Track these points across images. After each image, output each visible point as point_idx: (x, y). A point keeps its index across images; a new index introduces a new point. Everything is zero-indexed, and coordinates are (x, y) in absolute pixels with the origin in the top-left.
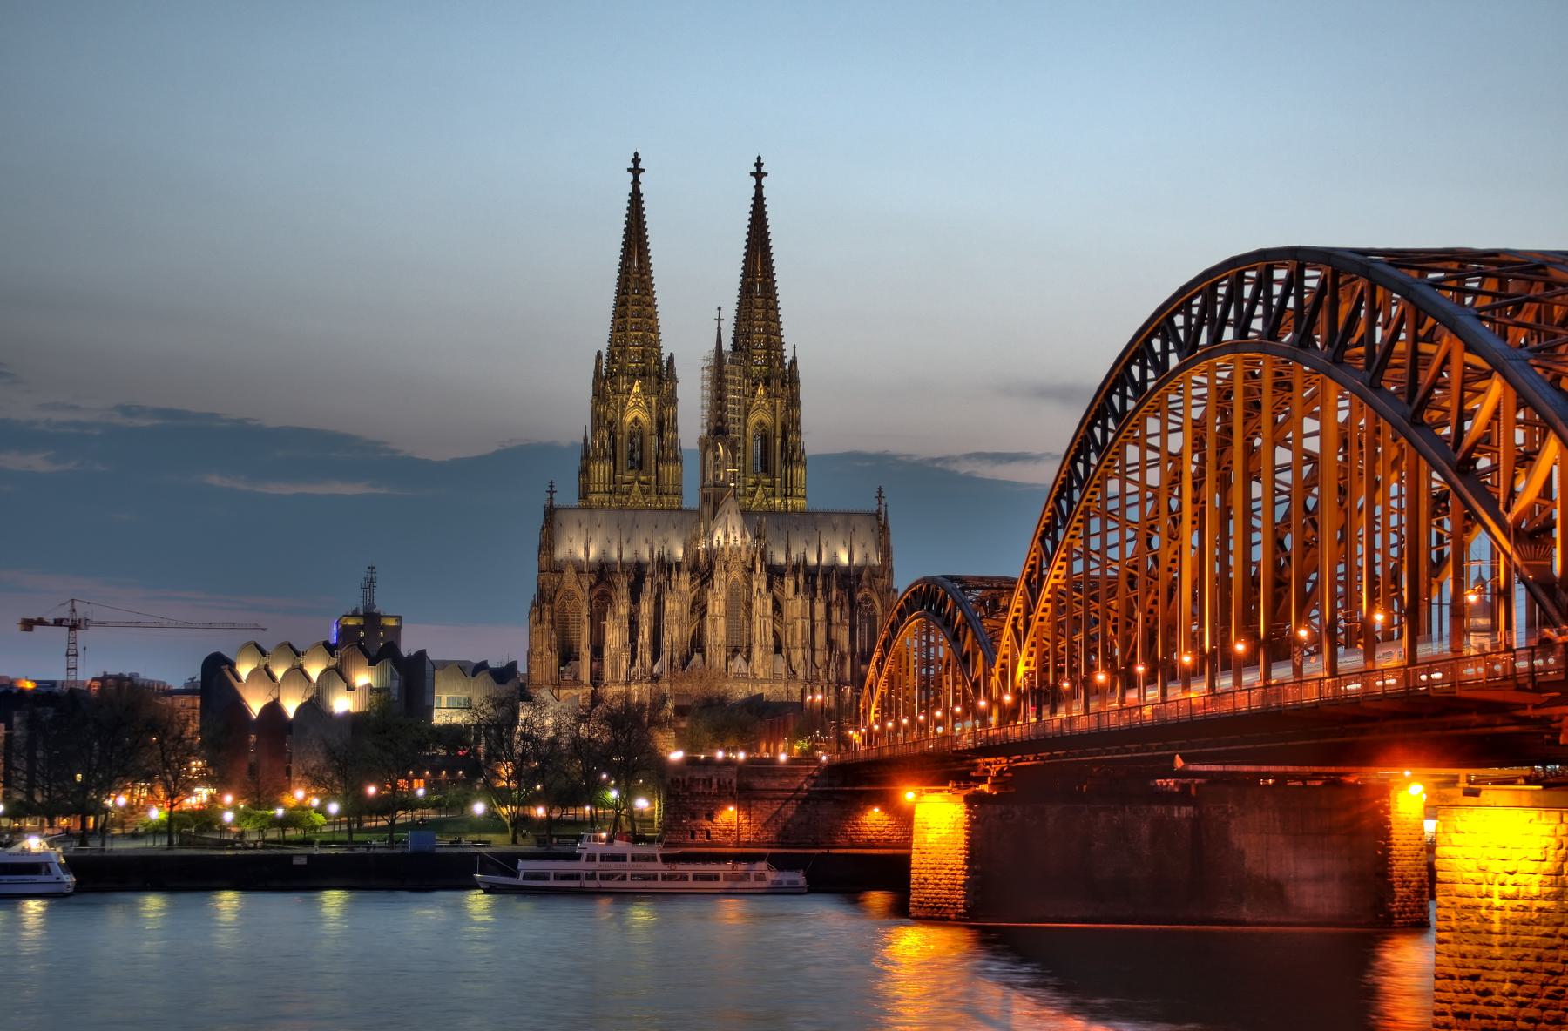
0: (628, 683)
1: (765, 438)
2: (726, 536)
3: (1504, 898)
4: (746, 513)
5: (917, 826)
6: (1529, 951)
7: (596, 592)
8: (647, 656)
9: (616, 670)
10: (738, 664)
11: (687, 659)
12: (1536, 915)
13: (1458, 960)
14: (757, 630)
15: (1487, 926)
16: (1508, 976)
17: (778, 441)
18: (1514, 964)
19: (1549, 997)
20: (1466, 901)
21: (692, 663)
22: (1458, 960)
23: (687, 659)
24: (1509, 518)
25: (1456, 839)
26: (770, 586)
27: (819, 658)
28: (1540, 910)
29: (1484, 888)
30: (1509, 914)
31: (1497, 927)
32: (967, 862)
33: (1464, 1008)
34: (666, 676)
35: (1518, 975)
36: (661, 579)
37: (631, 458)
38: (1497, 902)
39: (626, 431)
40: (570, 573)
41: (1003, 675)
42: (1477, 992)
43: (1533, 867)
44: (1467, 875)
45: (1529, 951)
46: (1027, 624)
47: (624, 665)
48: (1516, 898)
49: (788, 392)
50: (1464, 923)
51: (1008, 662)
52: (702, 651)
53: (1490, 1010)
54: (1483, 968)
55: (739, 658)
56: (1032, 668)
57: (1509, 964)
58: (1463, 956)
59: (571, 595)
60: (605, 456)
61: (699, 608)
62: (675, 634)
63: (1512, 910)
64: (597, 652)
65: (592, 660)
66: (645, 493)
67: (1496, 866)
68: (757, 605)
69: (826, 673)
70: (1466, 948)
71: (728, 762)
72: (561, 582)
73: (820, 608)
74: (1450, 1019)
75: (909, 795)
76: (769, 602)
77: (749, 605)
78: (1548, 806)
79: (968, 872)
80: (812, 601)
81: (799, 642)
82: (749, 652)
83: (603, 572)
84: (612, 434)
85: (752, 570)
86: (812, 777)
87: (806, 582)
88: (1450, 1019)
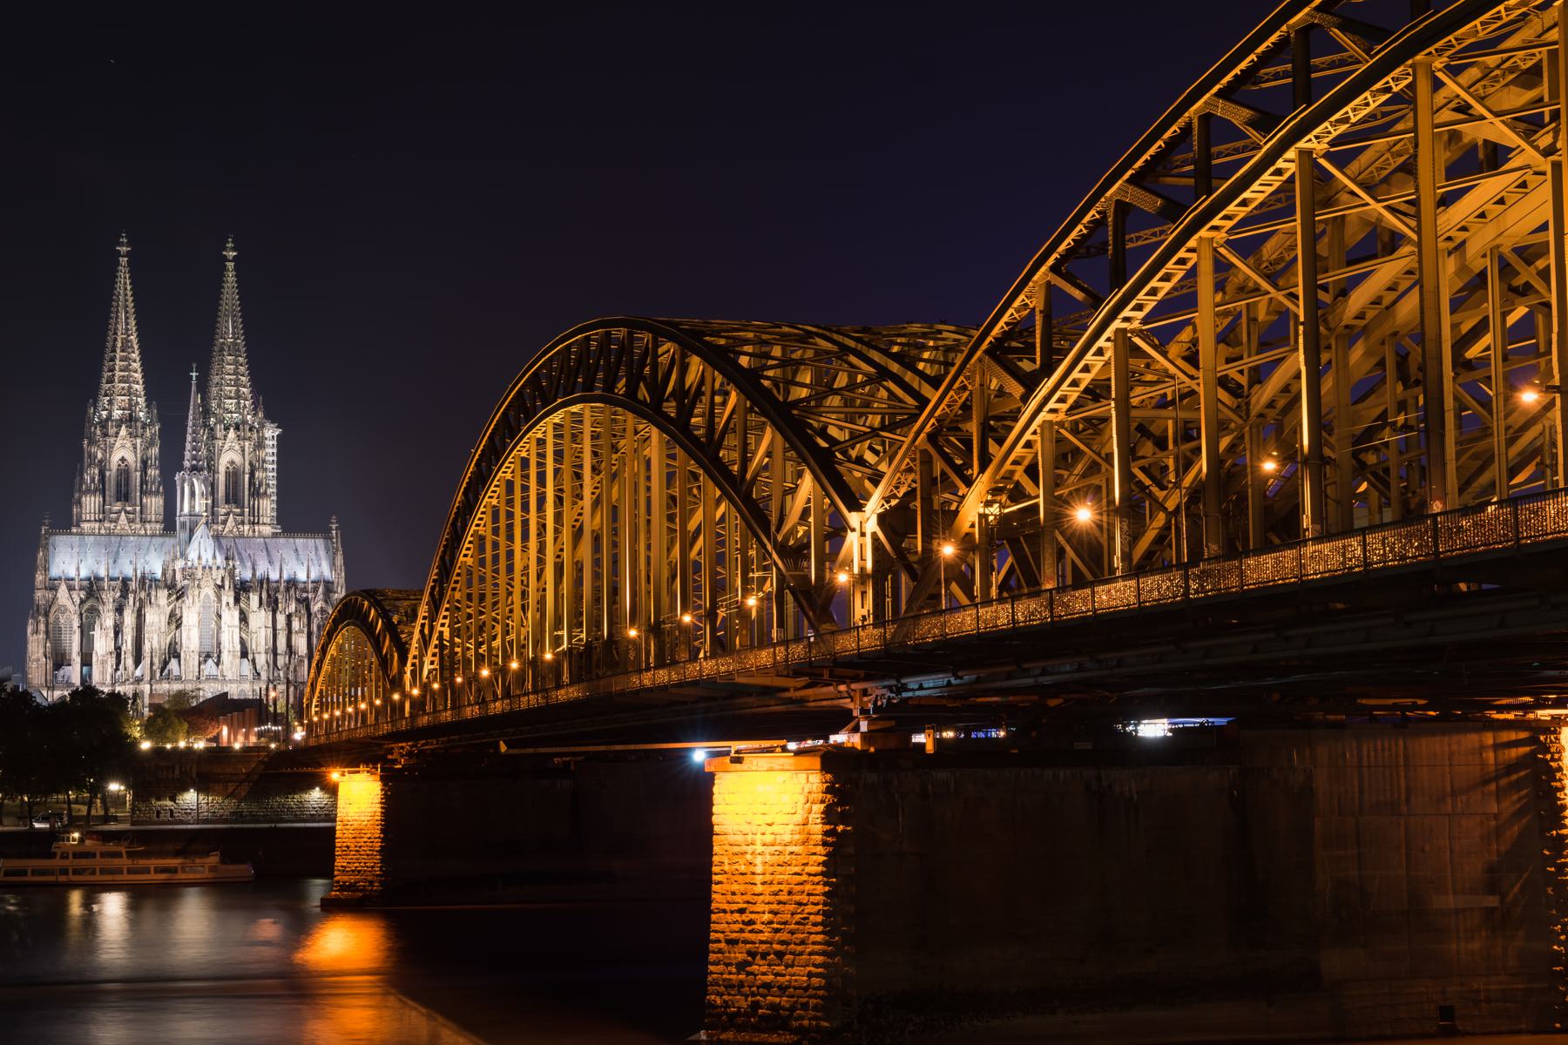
0: (113, 685)
4: (217, 538)
7: (86, 606)
8: (130, 662)
9: (103, 673)
14: (225, 638)
16: (767, 908)
18: (772, 898)
20: (736, 849)
21: (169, 666)
22: (729, 897)
23: (165, 663)
24: (780, 538)
25: (728, 798)
26: (237, 600)
27: (281, 661)
29: (749, 838)
30: (768, 858)
33: (734, 936)
34: (147, 678)
35: (775, 907)
37: (118, 491)
38: (759, 848)
39: (114, 467)
40: (63, 589)
41: (413, 673)
44: (736, 828)
47: (110, 670)
52: (178, 656)
57: (768, 898)
58: (734, 894)
59: (64, 610)
61: (175, 620)
62: (155, 640)
64: (87, 661)
65: (83, 665)
66: (131, 521)
67: (761, 820)
68: (225, 614)
69: (286, 674)
70: (735, 887)
73: (281, 619)
74: (723, 945)
75: (335, 775)
76: (236, 614)
77: (219, 616)
78: (798, 770)
80: (274, 612)
81: (262, 648)
83: (92, 588)
85: (221, 587)
87: (269, 596)
88: (723, 945)
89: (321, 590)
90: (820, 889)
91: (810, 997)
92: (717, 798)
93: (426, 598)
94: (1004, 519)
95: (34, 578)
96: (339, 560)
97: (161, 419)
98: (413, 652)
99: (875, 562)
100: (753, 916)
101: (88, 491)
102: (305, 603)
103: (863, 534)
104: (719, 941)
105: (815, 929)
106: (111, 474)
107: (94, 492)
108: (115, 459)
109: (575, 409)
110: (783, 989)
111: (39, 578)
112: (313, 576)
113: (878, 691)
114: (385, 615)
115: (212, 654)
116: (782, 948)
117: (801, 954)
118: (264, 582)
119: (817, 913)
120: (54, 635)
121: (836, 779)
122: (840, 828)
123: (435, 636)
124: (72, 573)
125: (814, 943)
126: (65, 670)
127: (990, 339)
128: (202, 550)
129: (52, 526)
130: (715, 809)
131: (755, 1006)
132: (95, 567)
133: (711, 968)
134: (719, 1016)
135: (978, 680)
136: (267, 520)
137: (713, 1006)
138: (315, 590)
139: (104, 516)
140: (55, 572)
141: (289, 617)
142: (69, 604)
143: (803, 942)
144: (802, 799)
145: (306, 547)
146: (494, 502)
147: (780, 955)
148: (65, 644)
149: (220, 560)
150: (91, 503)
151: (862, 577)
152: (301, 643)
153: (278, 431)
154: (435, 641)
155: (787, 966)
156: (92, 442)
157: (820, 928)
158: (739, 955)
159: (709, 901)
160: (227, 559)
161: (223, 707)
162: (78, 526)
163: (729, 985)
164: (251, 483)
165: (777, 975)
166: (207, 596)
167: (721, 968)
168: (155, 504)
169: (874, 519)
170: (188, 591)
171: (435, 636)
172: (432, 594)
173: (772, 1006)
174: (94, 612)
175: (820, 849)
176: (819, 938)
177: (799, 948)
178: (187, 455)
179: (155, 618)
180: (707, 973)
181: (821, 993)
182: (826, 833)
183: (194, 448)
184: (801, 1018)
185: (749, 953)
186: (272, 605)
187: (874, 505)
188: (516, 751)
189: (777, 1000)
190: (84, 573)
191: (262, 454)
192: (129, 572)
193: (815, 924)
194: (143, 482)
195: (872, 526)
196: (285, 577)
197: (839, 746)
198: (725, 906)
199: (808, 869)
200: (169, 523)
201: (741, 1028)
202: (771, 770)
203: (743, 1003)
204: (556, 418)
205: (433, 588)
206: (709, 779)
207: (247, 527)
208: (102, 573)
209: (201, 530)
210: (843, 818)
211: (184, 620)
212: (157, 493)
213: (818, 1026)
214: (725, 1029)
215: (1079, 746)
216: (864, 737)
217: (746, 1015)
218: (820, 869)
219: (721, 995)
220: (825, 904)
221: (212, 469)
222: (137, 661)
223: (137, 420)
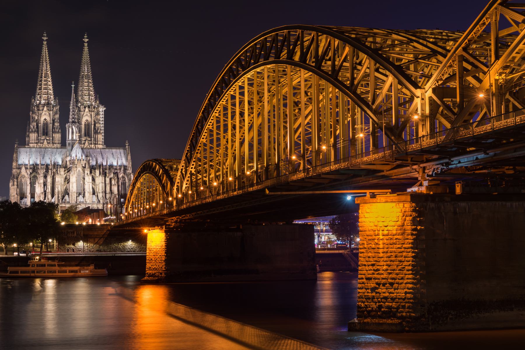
1: (88, 125)
2: (76, 156)
3: (383, 235)
4: (82, 149)
5: (148, 242)
6: (392, 254)
7: (32, 175)
8: (50, 196)
10: (81, 199)
11: (63, 197)
13: (367, 259)
14: (86, 187)
15: (378, 246)
16: (385, 263)
17: (93, 126)
19: (400, 270)
20: (370, 238)
21: (65, 198)
22: (367, 259)
23: (63, 197)
24: (374, 107)
25: (367, 215)
26: (91, 172)
27: (108, 196)
28: (396, 239)
30: (385, 241)
31: (381, 246)
32: (166, 253)
33: (370, 276)
36: (54, 170)
37: (44, 132)
38: (381, 237)
40: (23, 168)
41: (178, 189)
42: (374, 270)
43: (393, 224)
44: (370, 228)
45: (392, 254)
46: (186, 171)
48: (387, 235)
49: (96, 110)
50: (369, 246)
51: (179, 184)
52: (68, 194)
53: (378, 276)
54: (376, 261)
55: (81, 196)
56: (188, 185)
57: (385, 259)
58: (369, 257)
59: (24, 177)
60: (35, 131)
61: (67, 180)
62: (59, 188)
63: (387, 240)
64: (33, 196)
65: (31, 198)
66: (48, 143)
67: (381, 224)
70: (370, 254)
71: (80, 225)
72: (20, 172)
73: (108, 180)
74: (364, 280)
75: (145, 231)
76: (91, 178)
77: (84, 179)
78: (399, 202)
79: (166, 256)
81: (101, 191)
82: (84, 194)
83: (35, 168)
84: (37, 125)
85: (85, 167)
86: (108, 230)
87: (103, 171)
88: (364, 280)
89: (122, 169)
90: (410, 254)
91: (406, 303)
93: (184, 158)
94: (507, 82)
95: (12, 165)
96: (129, 157)
97: (59, 104)
98: (178, 180)
99: (431, 110)
100: (379, 267)
101: (32, 132)
102: (116, 174)
103: (423, 99)
104: (362, 279)
106: (41, 125)
107: (35, 131)
108: (42, 119)
109: (258, 70)
110: (393, 299)
111: (14, 164)
112: (119, 164)
113: (432, 168)
114: (163, 167)
115: (81, 193)
116: (393, 281)
118: (100, 166)
119: (409, 265)
120: (20, 186)
121: (417, 205)
122: (419, 227)
123: (189, 172)
124: (27, 163)
125: (408, 279)
126: (24, 200)
128: (77, 153)
129: (19, 144)
130: (360, 220)
131: (380, 307)
132: (35, 160)
134: (363, 312)
135: (495, 155)
136: (101, 143)
138: (120, 169)
139: (38, 141)
140: (20, 162)
141: (111, 179)
142: (26, 174)
143: (402, 278)
144: (401, 214)
145: (116, 153)
146: (217, 115)
147: (392, 284)
148: (24, 190)
149: (84, 157)
150: (33, 136)
151: (424, 117)
152: (115, 189)
153: (104, 109)
154: (188, 175)
155: (395, 289)
156: (34, 113)
160: (87, 156)
161: (88, 212)
162: (28, 145)
163: (368, 298)
164: (94, 128)
165: (390, 293)
166: (79, 171)
167: (364, 290)
168: (58, 136)
169: (431, 90)
170: (73, 168)
172: (186, 156)
174: (35, 178)
176: (410, 276)
177: (401, 281)
178: (71, 117)
179: (59, 179)
181: (411, 301)
182: (413, 230)
183: (73, 114)
184: (402, 312)
185: (377, 284)
186: (105, 175)
187: (430, 85)
188: (273, 193)
189: (391, 304)
190: (31, 163)
191: (99, 117)
192: (48, 162)
193: (408, 270)
194: (53, 128)
195: (429, 93)
196: (109, 164)
198: (366, 263)
199: (404, 246)
200: (63, 143)
201: (373, 317)
202: (387, 202)
203: (374, 306)
204: (249, 75)
205: (187, 154)
206: (356, 208)
207: (93, 146)
208: (38, 162)
209: (76, 146)
210: (420, 223)
211: (71, 180)
212: (58, 132)
213: (410, 315)
214: (366, 317)
217: (376, 311)
218: (410, 245)
219: (364, 302)
220: (412, 261)
221: (80, 123)
222: (53, 196)
223: (51, 104)
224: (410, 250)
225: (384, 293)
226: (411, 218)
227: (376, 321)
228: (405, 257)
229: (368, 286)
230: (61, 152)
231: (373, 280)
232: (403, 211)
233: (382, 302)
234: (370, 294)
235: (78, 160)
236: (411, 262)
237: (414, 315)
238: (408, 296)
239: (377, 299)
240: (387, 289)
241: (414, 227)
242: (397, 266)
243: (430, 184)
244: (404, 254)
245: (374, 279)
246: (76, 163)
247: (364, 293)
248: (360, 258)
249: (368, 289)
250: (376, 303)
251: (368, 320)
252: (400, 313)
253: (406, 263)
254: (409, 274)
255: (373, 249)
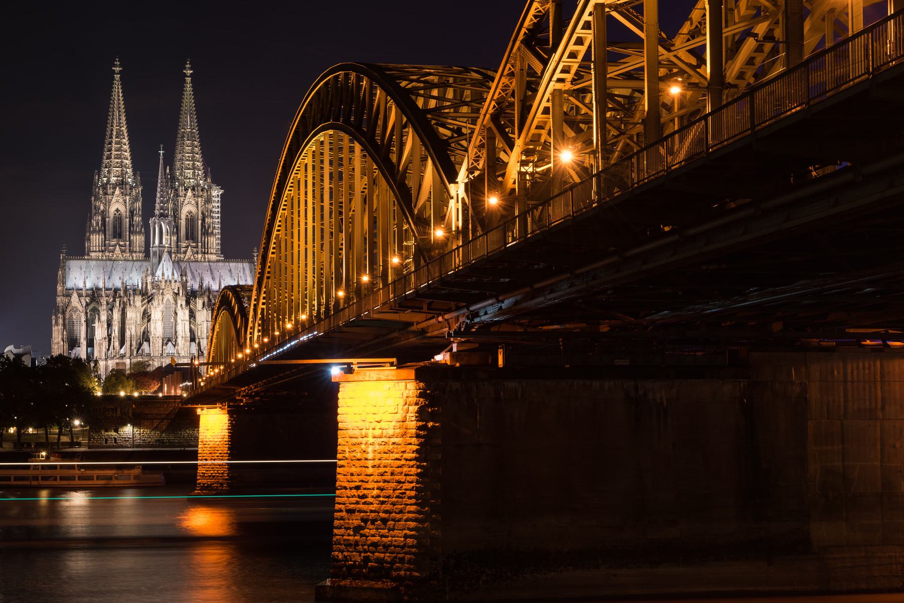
2: (163, 274)
6: (387, 469)
12: (391, 447)
13: (349, 477)
16: (376, 485)
18: (379, 478)
19: (397, 497)
20: (354, 441)
22: (349, 477)
25: (350, 402)
28: (394, 443)
30: (377, 447)
35: (381, 484)
38: (371, 440)
43: (389, 417)
44: (355, 424)
45: (387, 469)
50: (353, 454)
54: (363, 481)
57: (376, 478)
58: (352, 475)
67: (371, 418)
70: (353, 470)
74: (344, 514)
88: (344, 514)
90: (414, 470)
91: (406, 553)
92: (341, 402)
100: (366, 492)
104: (341, 511)
105: (410, 502)
110: (386, 547)
117: (399, 520)
119: (412, 489)
122: (430, 424)
125: (409, 512)
127: (523, 30)
128: (166, 270)
130: (339, 411)
131: (367, 560)
133: (335, 531)
134: (341, 567)
137: (336, 560)
143: (401, 512)
144: (402, 402)
147: (385, 521)
155: (389, 530)
157: (413, 501)
158: (355, 521)
159: (335, 480)
163: (348, 545)
165: (382, 536)
167: (342, 531)
171: (259, 311)
173: (380, 561)
175: (414, 440)
176: (413, 508)
177: (398, 516)
180: (332, 535)
181: (414, 550)
182: (419, 428)
184: (399, 569)
185: (363, 520)
189: (382, 555)
193: (410, 498)
197: (437, 363)
198: (346, 484)
199: (406, 456)
201: (356, 577)
202: (379, 380)
203: (358, 558)
209: (165, 256)
210: (433, 417)
213: (411, 575)
214: (344, 578)
215: (618, 362)
216: (454, 356)
217: (360, 567)
218: (414, 455)
219: (342, 551)
220: (417, 482)
224: (414, 462)
225: (373, 536)
226: (416, 407)
227: (359, 583)
228: (406, 475)
229: (348, 523)
230: (141, 267)
231: (357, 514)
232: (405, 395)
233: (369, 551)
234: (351, 538)
235: (166, 281)
236: (414, 484)
237: (417, 574)
238: (410, 541)
239: (363, 545)
240: (377, 529)
241: (420, 423)
242: (394, 490)
243: (461, 348)
244: (405, 469)
245: (358, 511)
246: (163, 287)
247: (343, 536)
248: (338, 476)
249: (349, 528)
250: (360, 552)
251: (347, 582)
252: (396, 570)
253: (407, 486)
254: (411, 505)
255: (359, 460)
